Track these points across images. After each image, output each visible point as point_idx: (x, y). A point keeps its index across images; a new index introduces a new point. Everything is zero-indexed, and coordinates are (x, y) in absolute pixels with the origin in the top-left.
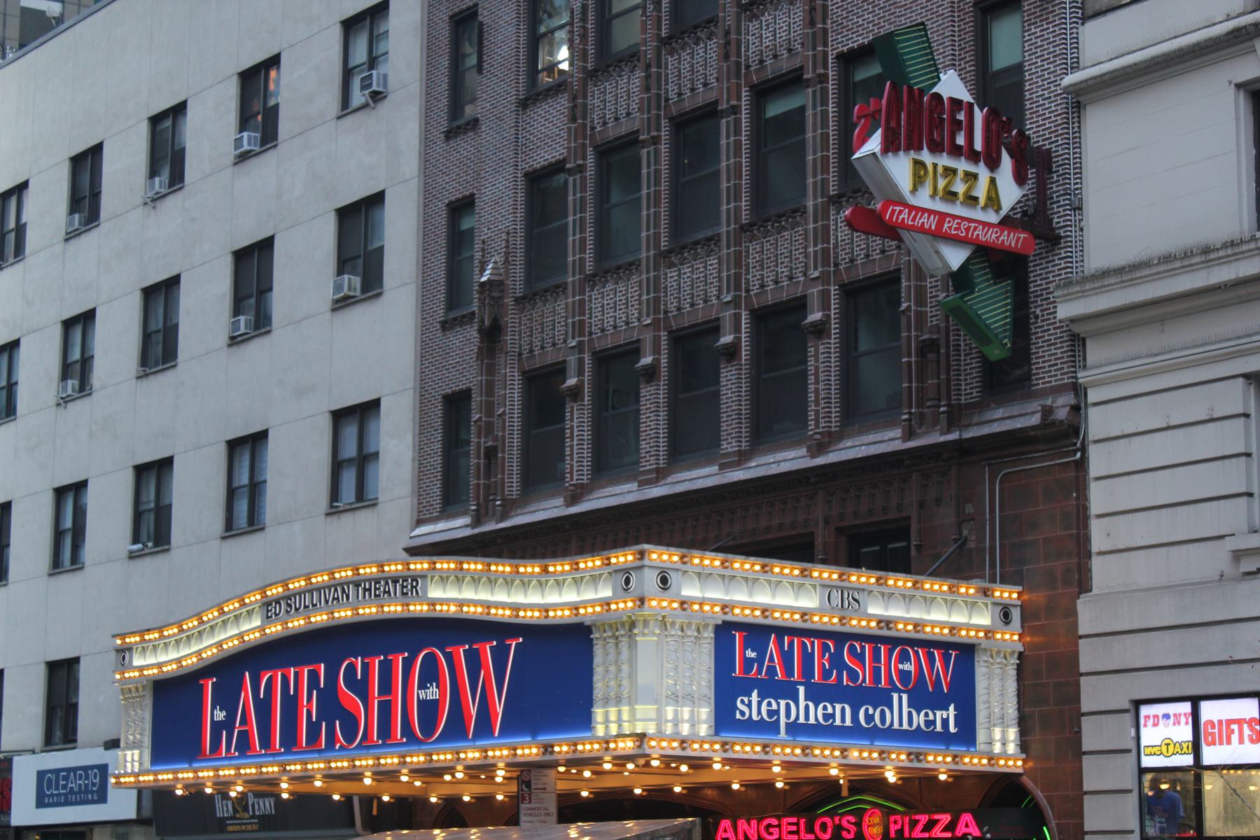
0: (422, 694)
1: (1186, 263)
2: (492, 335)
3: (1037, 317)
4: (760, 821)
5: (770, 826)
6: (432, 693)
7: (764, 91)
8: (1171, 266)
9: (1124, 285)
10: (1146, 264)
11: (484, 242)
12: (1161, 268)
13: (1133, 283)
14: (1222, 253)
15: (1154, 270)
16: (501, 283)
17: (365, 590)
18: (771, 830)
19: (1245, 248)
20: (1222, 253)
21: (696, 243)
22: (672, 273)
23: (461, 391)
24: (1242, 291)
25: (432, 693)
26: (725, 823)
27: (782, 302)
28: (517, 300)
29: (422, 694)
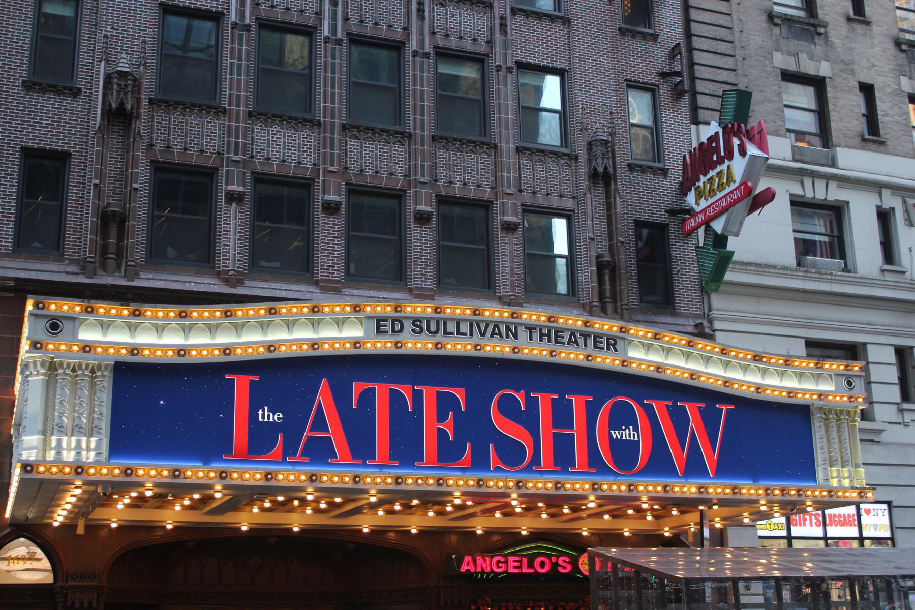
0: (615, 434)
1: (794, 273)
2: (119, 118)
3: (678, 271)
4: (492, 557)
5: (499, 562)
6: (628, 434)
7: (443, 54)
8: (786, 272)
9: (757, 273)
10: (775, 267)
11: (106, 36)
12: (781, 272)
13: (763, 273)
14: (813, 275)
15: (777, 271)
16: (135, 80)
17: (541, 335)
18: (500, 565)
19: (825, 276)
20: (813, 275)
21: (382, 130)
22: (353, 144)
23: (55, 152)
24: (808, 296)
25: (628, 434)
26: (467, 558)
27: (469, 199)
28: (151, 101)
29: (615, 434)
